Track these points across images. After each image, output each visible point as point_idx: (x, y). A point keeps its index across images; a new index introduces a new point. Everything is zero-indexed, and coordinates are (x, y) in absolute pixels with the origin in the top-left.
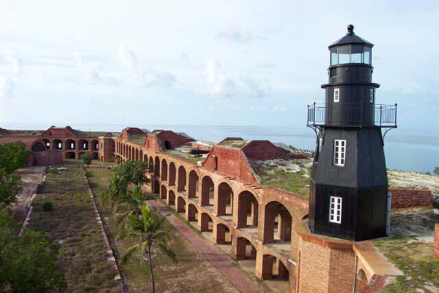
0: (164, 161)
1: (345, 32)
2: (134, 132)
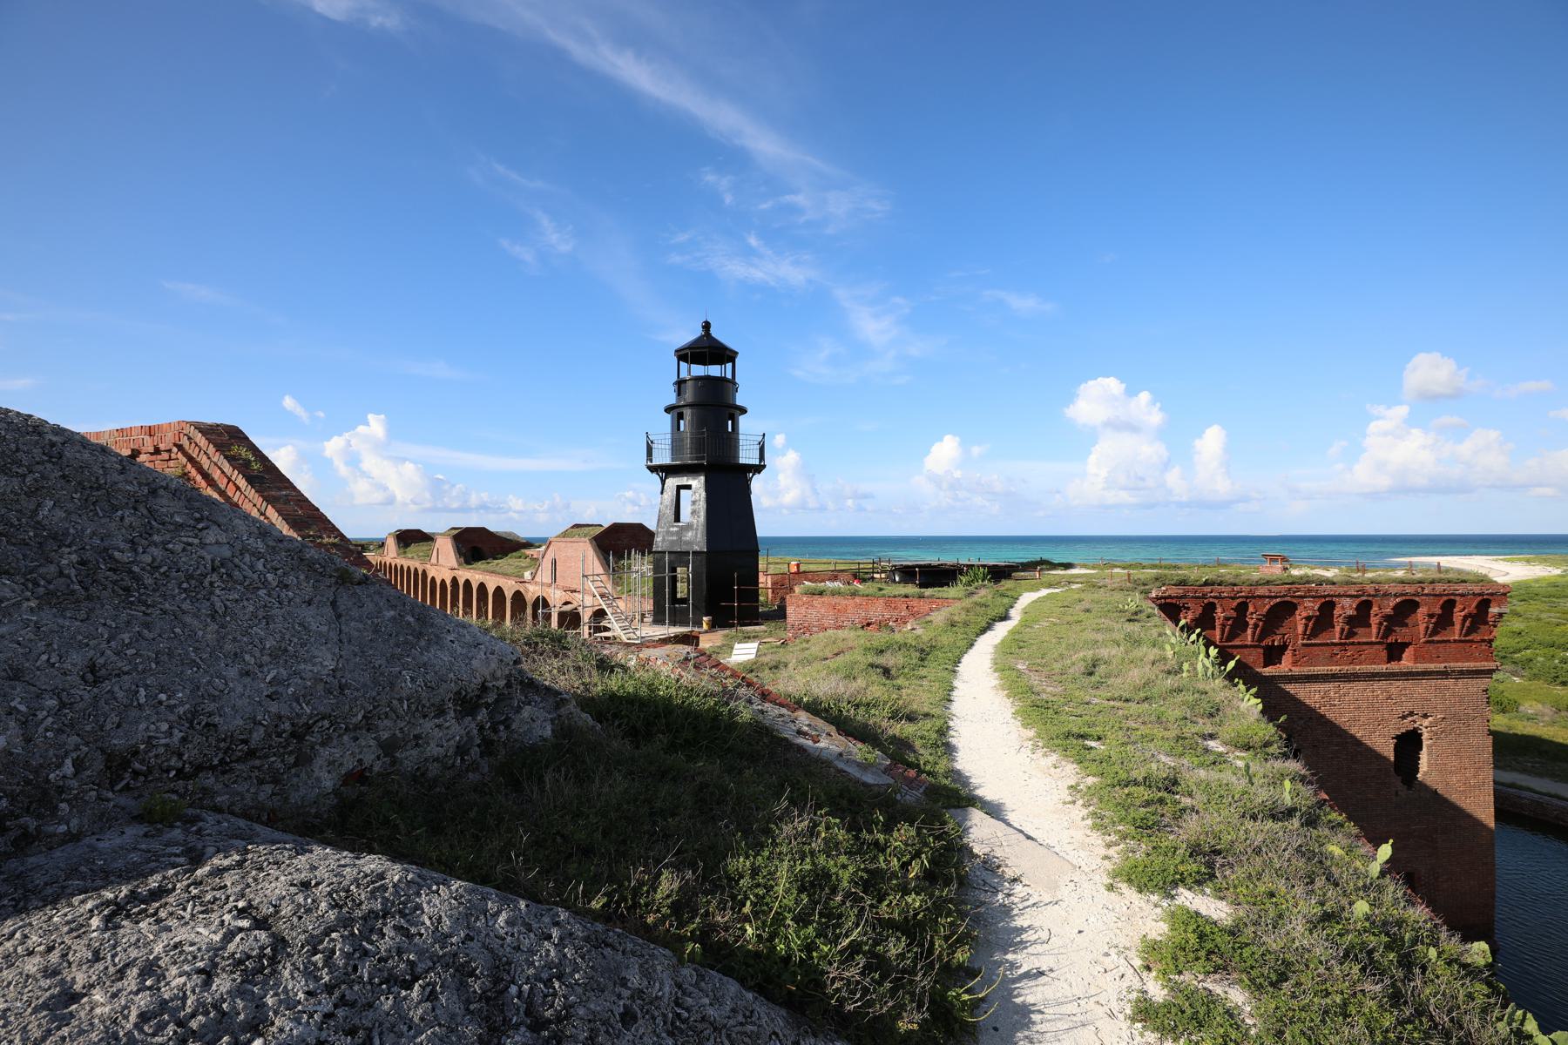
0: (467, 583)
1: (699, 332)
2: (408, 538)
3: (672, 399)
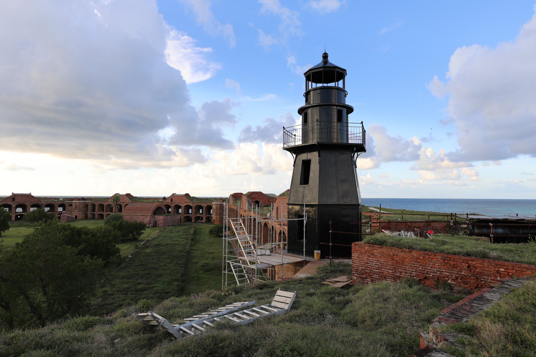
2: (237, 197)
3: (303, 104)
